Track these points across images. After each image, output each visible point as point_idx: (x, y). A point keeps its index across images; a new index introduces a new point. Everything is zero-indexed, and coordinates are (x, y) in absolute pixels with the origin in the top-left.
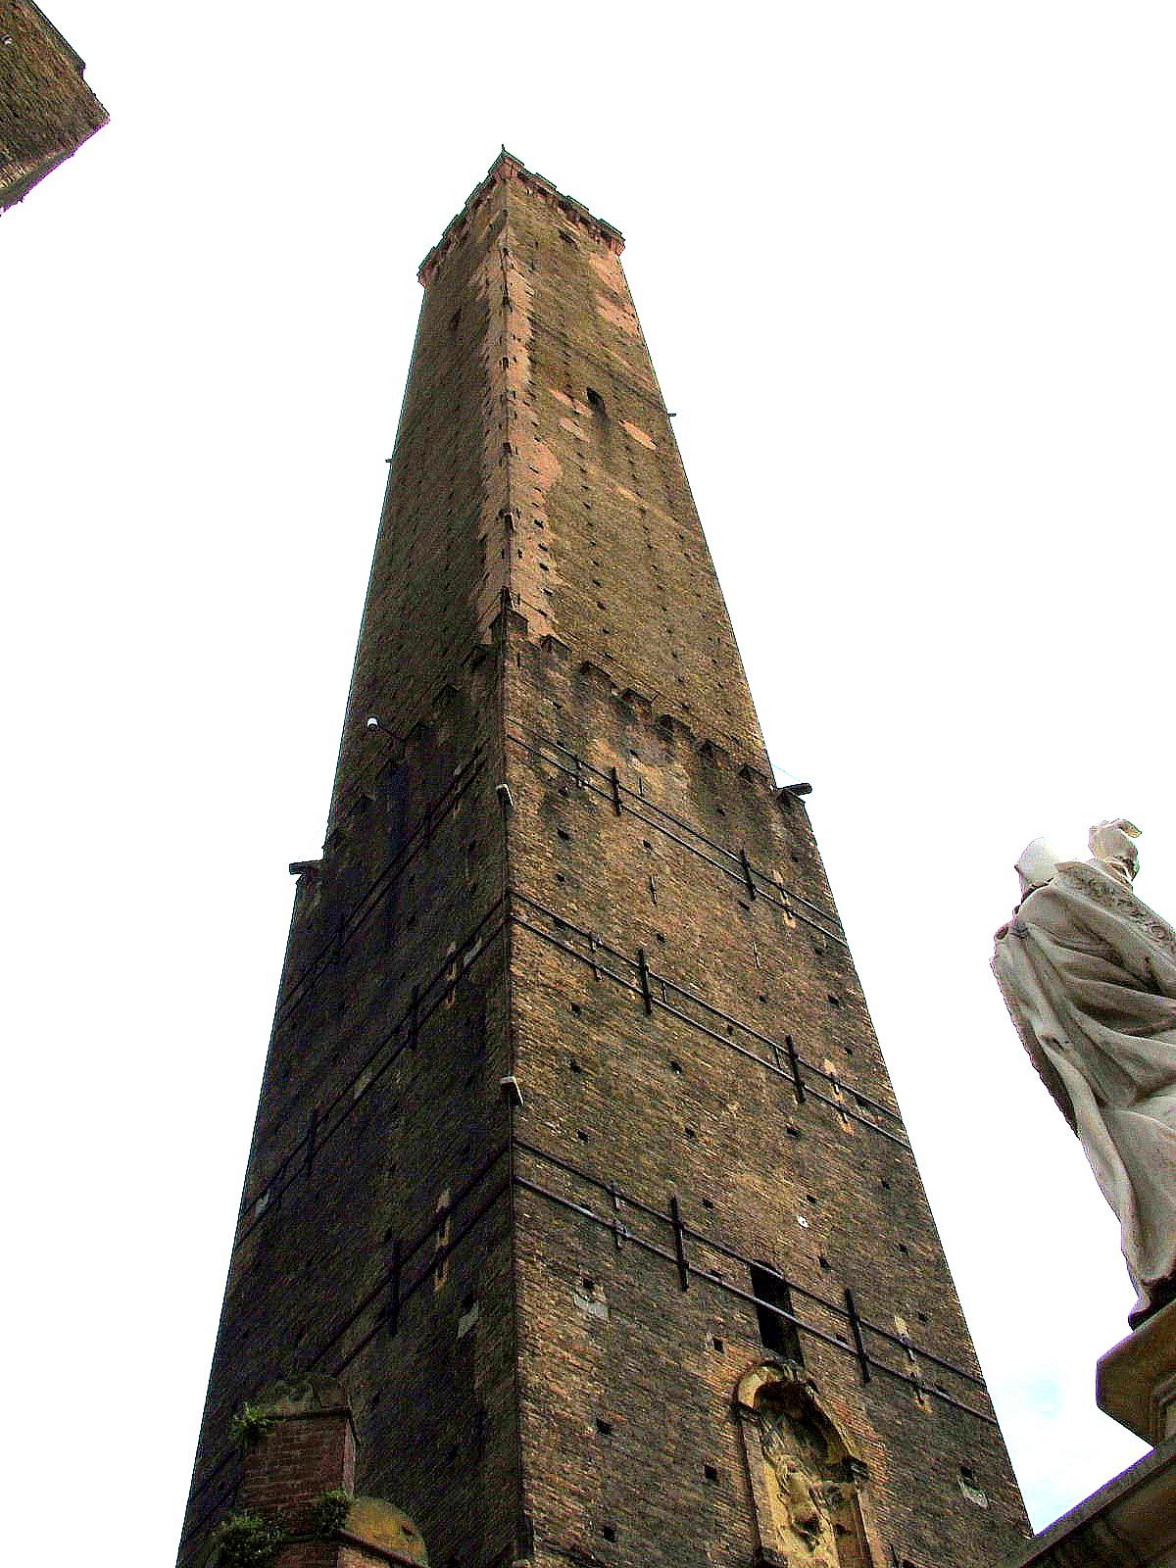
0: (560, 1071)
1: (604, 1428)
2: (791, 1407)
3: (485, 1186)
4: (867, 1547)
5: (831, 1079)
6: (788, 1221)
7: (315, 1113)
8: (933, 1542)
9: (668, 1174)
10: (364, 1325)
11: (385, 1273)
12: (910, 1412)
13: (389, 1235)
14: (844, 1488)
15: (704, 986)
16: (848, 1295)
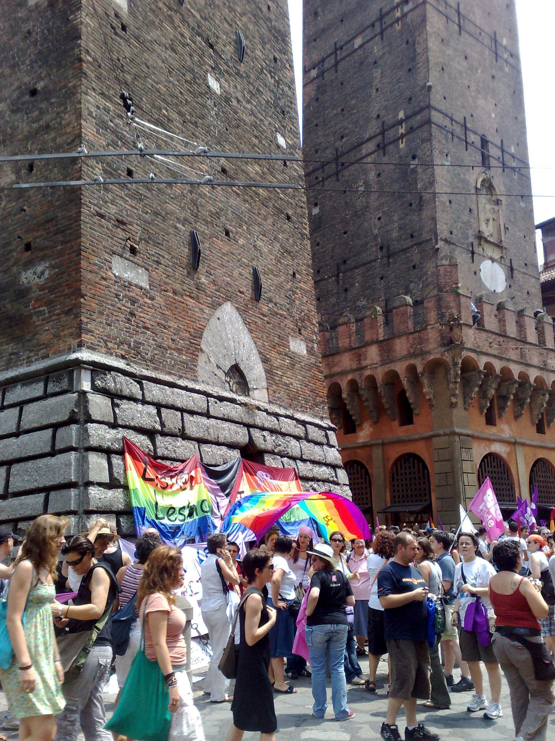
0: (439, 72)
1: (450, 202)
2: (489, 186)
3: (418, 117)
4: (500, 225)
5: (505, 48)
6: (490, 117)
7: (336, 44)
8: (513, 220)
9: (464, 107)
10: (371, 146)
11: (378, 131)
12: (512, 180)
13: (378, 116)
14: (496, 208)
15: (474, 14)
16: (502, 141)
